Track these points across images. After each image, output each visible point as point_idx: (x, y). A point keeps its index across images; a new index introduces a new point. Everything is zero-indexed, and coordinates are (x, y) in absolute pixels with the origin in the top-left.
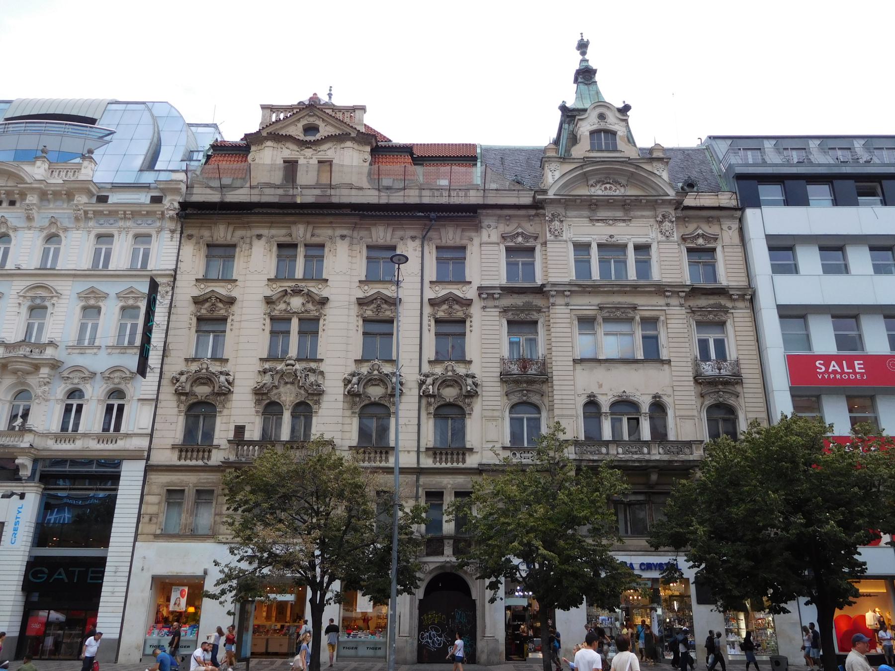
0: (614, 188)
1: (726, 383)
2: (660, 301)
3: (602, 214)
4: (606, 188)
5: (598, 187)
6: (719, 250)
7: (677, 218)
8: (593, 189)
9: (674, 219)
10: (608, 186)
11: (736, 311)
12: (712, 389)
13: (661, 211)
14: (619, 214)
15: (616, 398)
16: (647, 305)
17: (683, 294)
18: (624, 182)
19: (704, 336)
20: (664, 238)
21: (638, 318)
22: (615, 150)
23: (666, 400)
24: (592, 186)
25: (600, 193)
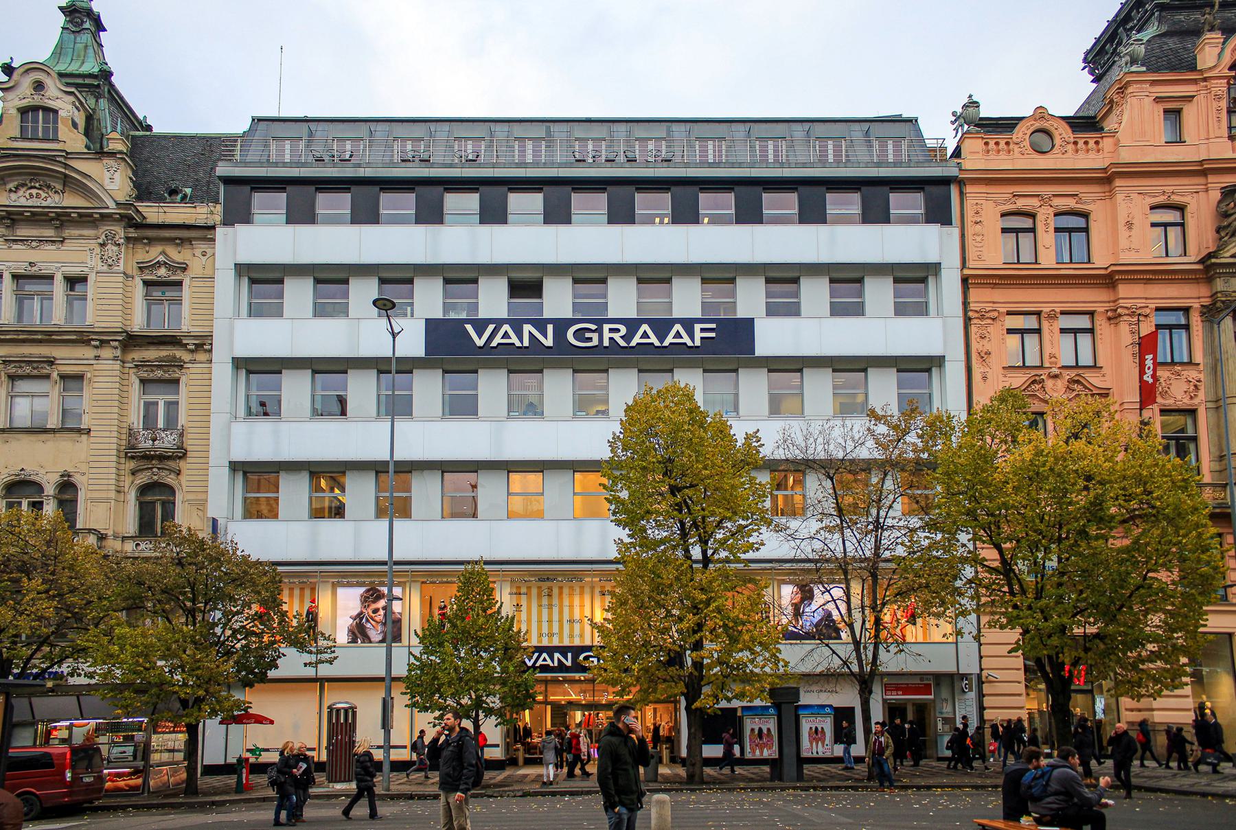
0: (44, 195)
1: (162, 458)
2: (89, 352)
3: (23, 232)
4: (31, 195)
5: (21, 193)
6: (186, 283)
7: (128, 239)
8: (13, 196)
9: (122, 241)
10: (34, 192)
11: (194, 365)
12: (144, 464)
13: (104, 229)
14: (49, 233)
15: (13, 477)
16: (68, 357)
17: (116, 344)
18: (59, 187)
19: (150, 398)
20: (105, 268)
21: (55, 375)
22: (56, 140)
23: (77, 479)
24: (11, 191)
25: (23, 202)
